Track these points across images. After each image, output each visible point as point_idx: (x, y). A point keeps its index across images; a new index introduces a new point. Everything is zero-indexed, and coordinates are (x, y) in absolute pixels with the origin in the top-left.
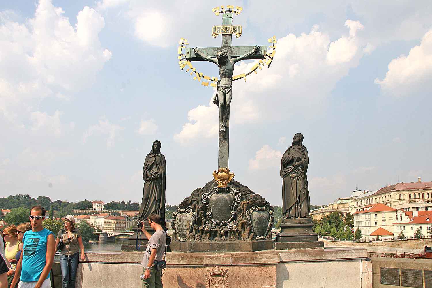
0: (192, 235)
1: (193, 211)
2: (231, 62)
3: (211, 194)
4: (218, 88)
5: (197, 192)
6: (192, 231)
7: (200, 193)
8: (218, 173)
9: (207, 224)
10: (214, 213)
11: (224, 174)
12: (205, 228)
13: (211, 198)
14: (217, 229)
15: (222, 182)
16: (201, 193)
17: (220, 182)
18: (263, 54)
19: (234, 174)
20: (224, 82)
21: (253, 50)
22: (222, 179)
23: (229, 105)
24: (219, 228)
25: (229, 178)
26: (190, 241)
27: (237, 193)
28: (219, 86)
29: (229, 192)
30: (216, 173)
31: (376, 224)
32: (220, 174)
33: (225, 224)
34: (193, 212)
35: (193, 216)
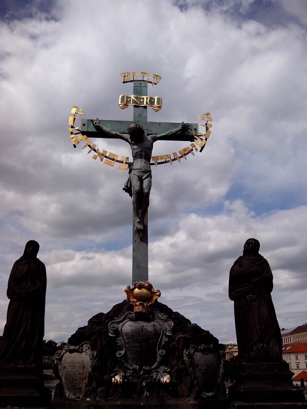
0: (91, 389)
1: (93, 348)
2: (149, 139)
3: (124, 322)
4: (130, 173)
5: (99, 321)
6: (89, 384)
7: (104, 321)
8: (134, 289)
9: (117, 370)
10: (128, 353)
11: (144, 291)
12: (115, 379)
13: (123, 329)
14: (136, 381)
15: (140, 304)
16: (107, 321)
17: (137, 304)
18: (194, 134)
19: (159, 291)
20: (139, 164)
21: (180, 128)
22: (140, 298)
23: (148, 194)
24: (138, 378)
25: (152, 297)
26: (88, 399)
27: (166, 321)
28: (132, 169)
29: (153, 320)
30: (131, 290)
31: (298, 367)
32: (137, 290)
33: (150, 372)
34: (92, 351)
35: (93, 358)
